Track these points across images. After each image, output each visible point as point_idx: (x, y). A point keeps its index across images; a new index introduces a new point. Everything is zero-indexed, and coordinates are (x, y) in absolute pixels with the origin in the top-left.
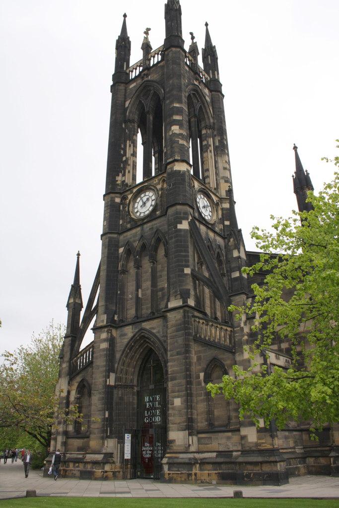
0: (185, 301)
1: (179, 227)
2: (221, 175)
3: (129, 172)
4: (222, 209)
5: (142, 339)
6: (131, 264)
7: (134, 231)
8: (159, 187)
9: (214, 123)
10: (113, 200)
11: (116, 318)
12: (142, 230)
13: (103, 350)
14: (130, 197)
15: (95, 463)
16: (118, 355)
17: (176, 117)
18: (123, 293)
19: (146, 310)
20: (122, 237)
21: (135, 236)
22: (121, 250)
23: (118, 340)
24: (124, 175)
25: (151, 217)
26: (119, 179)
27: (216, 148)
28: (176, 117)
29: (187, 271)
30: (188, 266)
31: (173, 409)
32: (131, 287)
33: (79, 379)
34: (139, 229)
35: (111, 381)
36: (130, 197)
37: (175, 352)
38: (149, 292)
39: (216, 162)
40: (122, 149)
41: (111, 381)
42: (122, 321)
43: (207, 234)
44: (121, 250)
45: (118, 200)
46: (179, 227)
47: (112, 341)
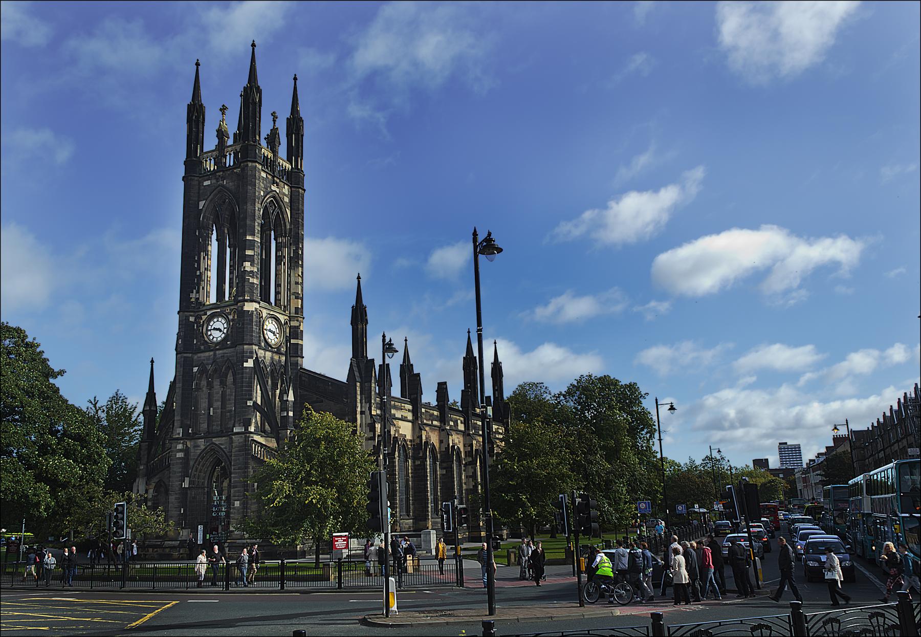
0: (247, 429)
1: (245, 365)
3: (203, 288)
4: (290, 327)
5: (212, 449)
6: (204, 383)
7: (207, 354)
8: (231, 317)
9: (290, 229)
10: (187, 318)
12: (215, 355)
13: (179, 458)
14: (204, 317)
15: (174, 547)
16: (192, 463)
17: (249, 252)
18: (197, 409)
19: (216, 428)
20: (195, 357)
21: (208, 358)
22: (195, 369)
23: (192, 450)
24: (198, 292)
25: (222, 344)
26: (193, 296)
27: (290, 259)
28: (249, 252)
29: (250, 403)
30: (251, 399)
31: (234, 508)
32: (204, 404)
33: (155, 480)
34: (212, 353)
35: (186, 484)
36: (204, 317)
37: (237, 467)
38: (219, 411)
39: (289, 275)
40: (196, 261)
41: (186, 484)
42: (194, 433)
44: (195, 369)
45: (192, 319)
46: (245, 365)
47: (186, 451)
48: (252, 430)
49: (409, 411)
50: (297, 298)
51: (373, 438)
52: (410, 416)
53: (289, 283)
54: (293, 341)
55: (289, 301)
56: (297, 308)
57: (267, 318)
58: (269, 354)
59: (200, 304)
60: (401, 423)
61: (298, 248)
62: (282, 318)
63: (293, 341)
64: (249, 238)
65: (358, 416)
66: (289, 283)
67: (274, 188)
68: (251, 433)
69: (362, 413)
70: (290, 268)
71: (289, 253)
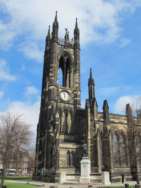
1: (49, 108)
2: (75, 81)
11: (42, 134)
26: (44, 90)
28: (51, 70)
29: (50, 121)
30: (50, 120)
43: (64, 105)
45: (44, 97)
46: (49, 108)
48: (51, 131)
49: (125, 119)
50: (76, 83)
51: (95, 131)
52: (126, 122)
53: (74, 79)
54: (75, 99)
55: (74, 85)
56: (76, 87)
57: (61, 92)
58: (62, 104)
59: (46, 92)
60: (119, 125)
61: (76, 67)
62: (70, 92)
63: (75, 99)
64: (51, 65)
65: (89, 122)
66: (74, 79)
67: (65, 50)
68: (50, 132)
69: (91, 120)
70: (74, 74)
71: (73, 69)
